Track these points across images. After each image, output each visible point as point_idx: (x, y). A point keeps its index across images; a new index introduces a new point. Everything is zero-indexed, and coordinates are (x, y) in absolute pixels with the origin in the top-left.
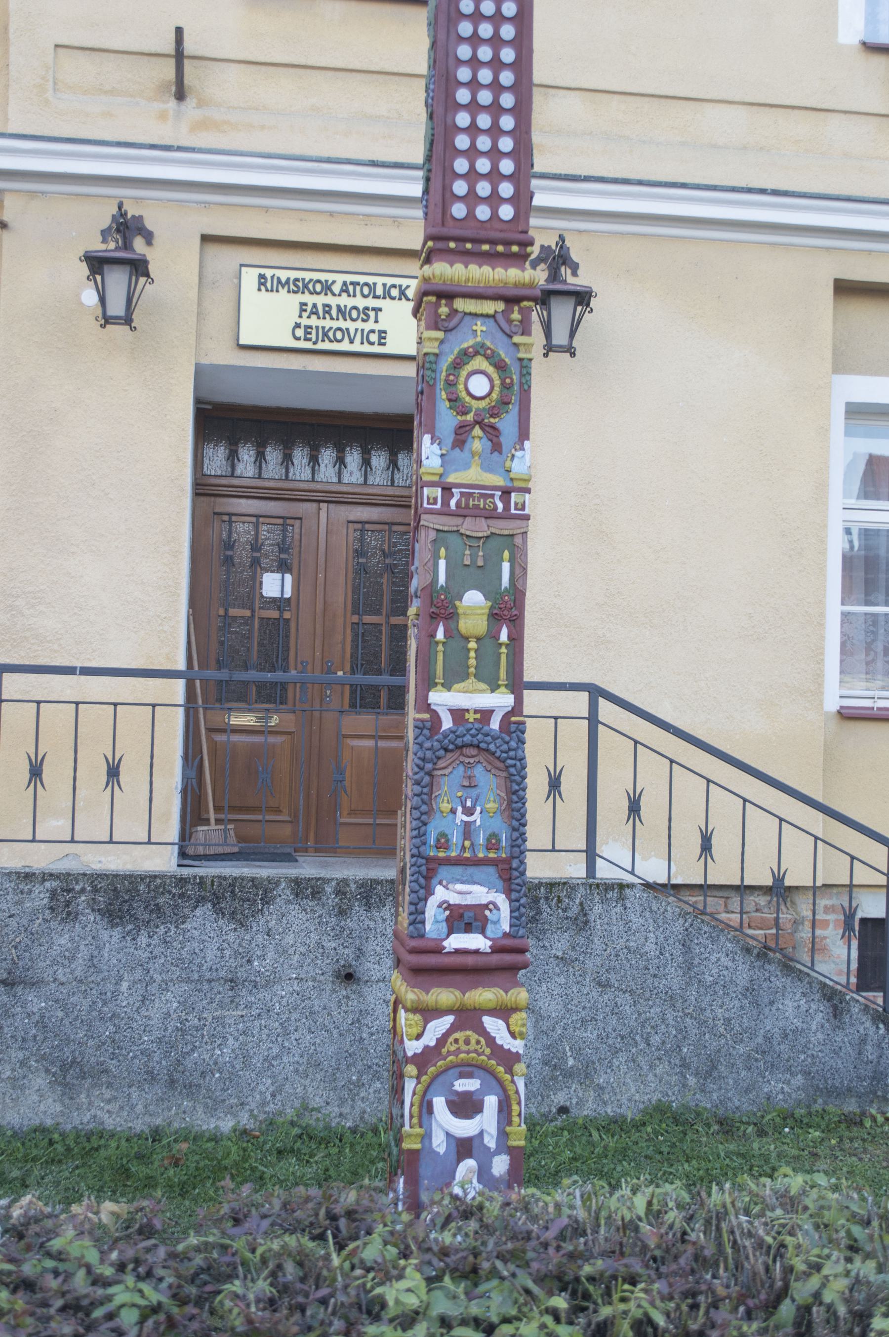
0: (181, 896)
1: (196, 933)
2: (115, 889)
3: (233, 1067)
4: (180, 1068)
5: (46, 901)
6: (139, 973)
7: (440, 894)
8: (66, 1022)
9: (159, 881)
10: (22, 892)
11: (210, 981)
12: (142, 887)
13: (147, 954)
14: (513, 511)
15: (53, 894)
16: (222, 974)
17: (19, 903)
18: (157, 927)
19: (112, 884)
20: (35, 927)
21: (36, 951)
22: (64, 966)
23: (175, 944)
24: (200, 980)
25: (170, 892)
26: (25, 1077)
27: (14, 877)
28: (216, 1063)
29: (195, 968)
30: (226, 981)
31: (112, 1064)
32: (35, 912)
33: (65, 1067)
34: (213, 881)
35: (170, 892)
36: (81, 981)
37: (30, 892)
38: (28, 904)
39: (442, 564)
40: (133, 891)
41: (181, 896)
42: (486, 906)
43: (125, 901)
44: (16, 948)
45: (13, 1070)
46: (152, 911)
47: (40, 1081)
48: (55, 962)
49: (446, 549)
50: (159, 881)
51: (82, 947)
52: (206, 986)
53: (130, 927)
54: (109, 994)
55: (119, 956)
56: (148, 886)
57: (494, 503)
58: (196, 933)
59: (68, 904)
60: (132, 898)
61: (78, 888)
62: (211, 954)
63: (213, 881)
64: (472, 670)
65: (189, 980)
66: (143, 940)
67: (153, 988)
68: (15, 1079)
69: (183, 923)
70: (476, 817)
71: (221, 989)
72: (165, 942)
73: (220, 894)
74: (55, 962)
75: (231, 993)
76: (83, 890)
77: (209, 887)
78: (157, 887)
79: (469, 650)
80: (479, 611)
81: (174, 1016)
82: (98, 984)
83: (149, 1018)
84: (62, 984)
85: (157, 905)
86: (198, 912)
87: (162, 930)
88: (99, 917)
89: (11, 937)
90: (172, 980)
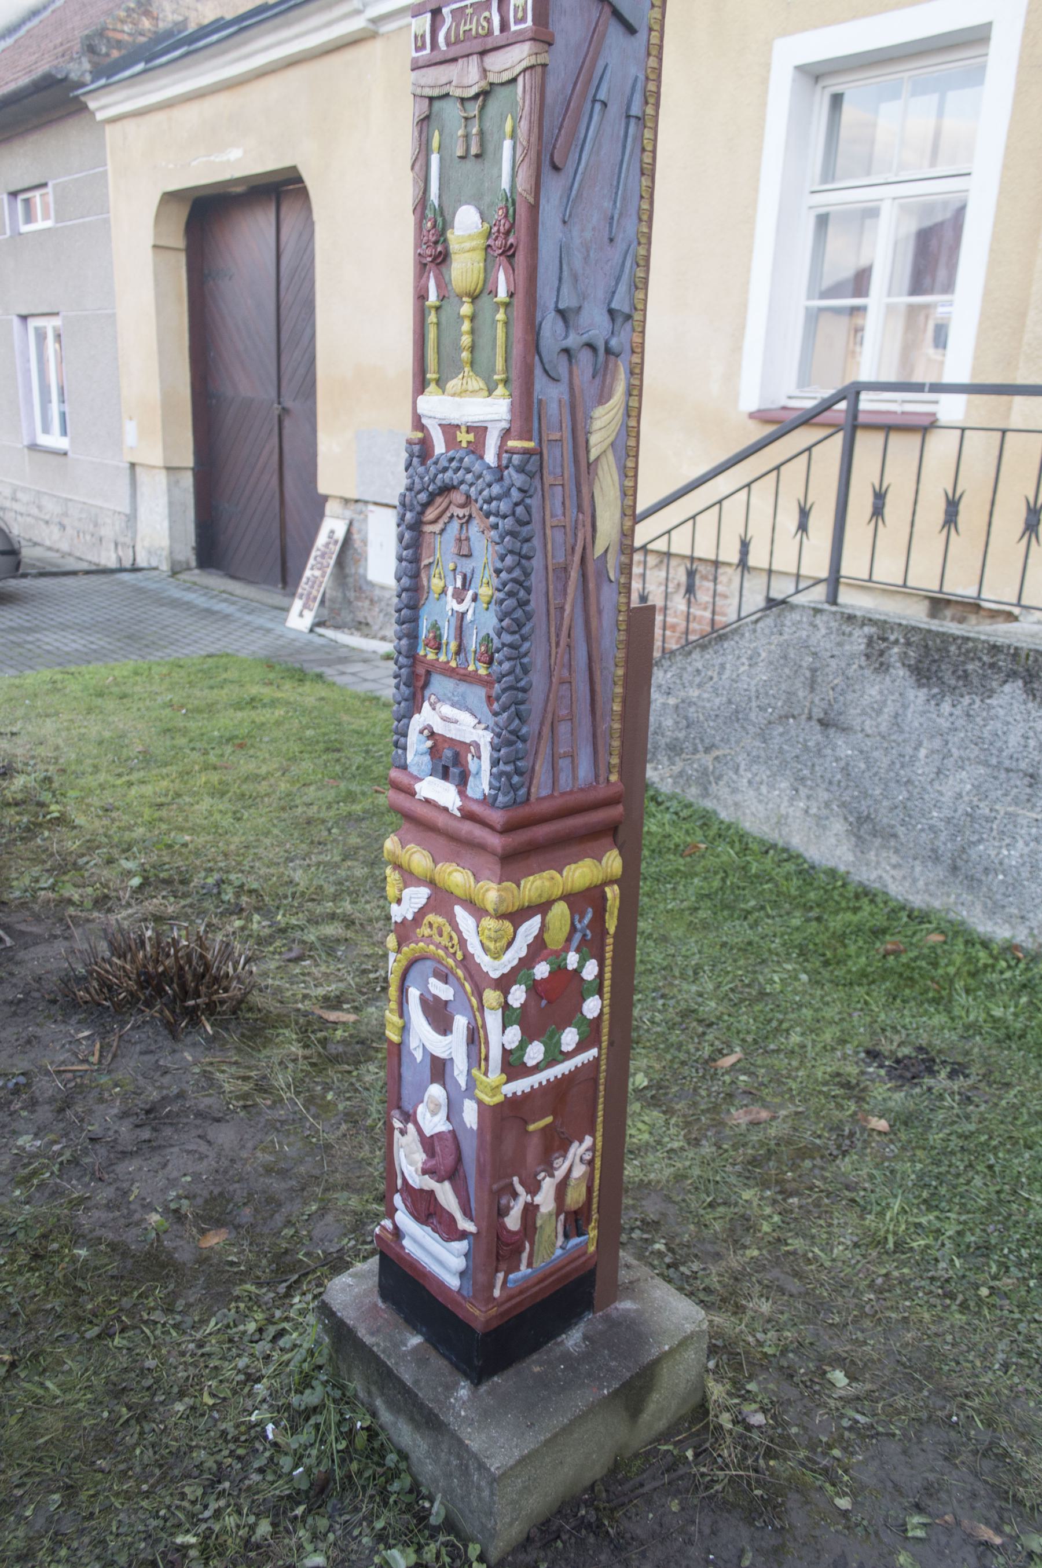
0: (992, 666)
1: (1002, 712)
2: (926, 646)
3: (1019, 874)
4: (964, 857)
5: (863, 647)
6: (937, 743)
7: (426, 716)
8: (867, 775)
9: (971, 644)
10: (844, 634)
11: (1008, 770)
12: (953, 648)
13: (948, 725)
14: (514, 28)
15: (870, 642)
16: (1023, 765)
17: (840, 644)
18: (962, 696)
19: (924, 639)
20: (850, 672)
21: (850, 696)
22: (871, 717)
23: (978, 719)
24: (998, 767)
25: (980, 659)
26: (827, 818)
27: (838, 617)
28: (1001, 863)
29: (994, 752)
30: (1026, 775)
31: (901, 831)
32: (853, 656)
33: (863, 819)
34: (1028, 656)
35: (980, 659)
36: (883, 737)
37: (850, 634)
38: (847, 647)
39: (435, 159)
40: (944, 650)
41: (992, 666)
42: (467, 746)
43: (935, 661)
44: (833, 689)
45: (819, 808)
46: (959, 678)
47: (838, 826)
48: (864, 713)
49: (440, 135)
50: (971, 644)
51: (889, 702)
52: (1003, 775)
53: (935, 690)
54: (907, 758)
55: (922, 720)
56: (959, 648)
57: (488, 20)
58: (1002, 712)
59: (882, 653)
60: (941, 659)
61: (892, 638)
62: (1014, 740)
63: (1028, 656)
64: (465, 355)
65: (986, 764)
66: (946, 707)
67: (949, 763)
68: (820, 818)
69: (989, 697)
70: (467, 604)
71: (1019, 783)
72: (968, 715)
73: (1034, 672)
74: (864, 713)
75: (1028, 790)
76: (896, 642)
77: (1023, 661)
78: (968, 651)
79: (461, 318)
80: (468, 245)
81: (966, 799)
82: (899, 744)
83: (941, 794)
84: (868, 736)
85: (965, 671)
86: (1007, 688)
87: (966, 700)
88: (908, 673)
89: (831, 677)
90: (969, 759)
